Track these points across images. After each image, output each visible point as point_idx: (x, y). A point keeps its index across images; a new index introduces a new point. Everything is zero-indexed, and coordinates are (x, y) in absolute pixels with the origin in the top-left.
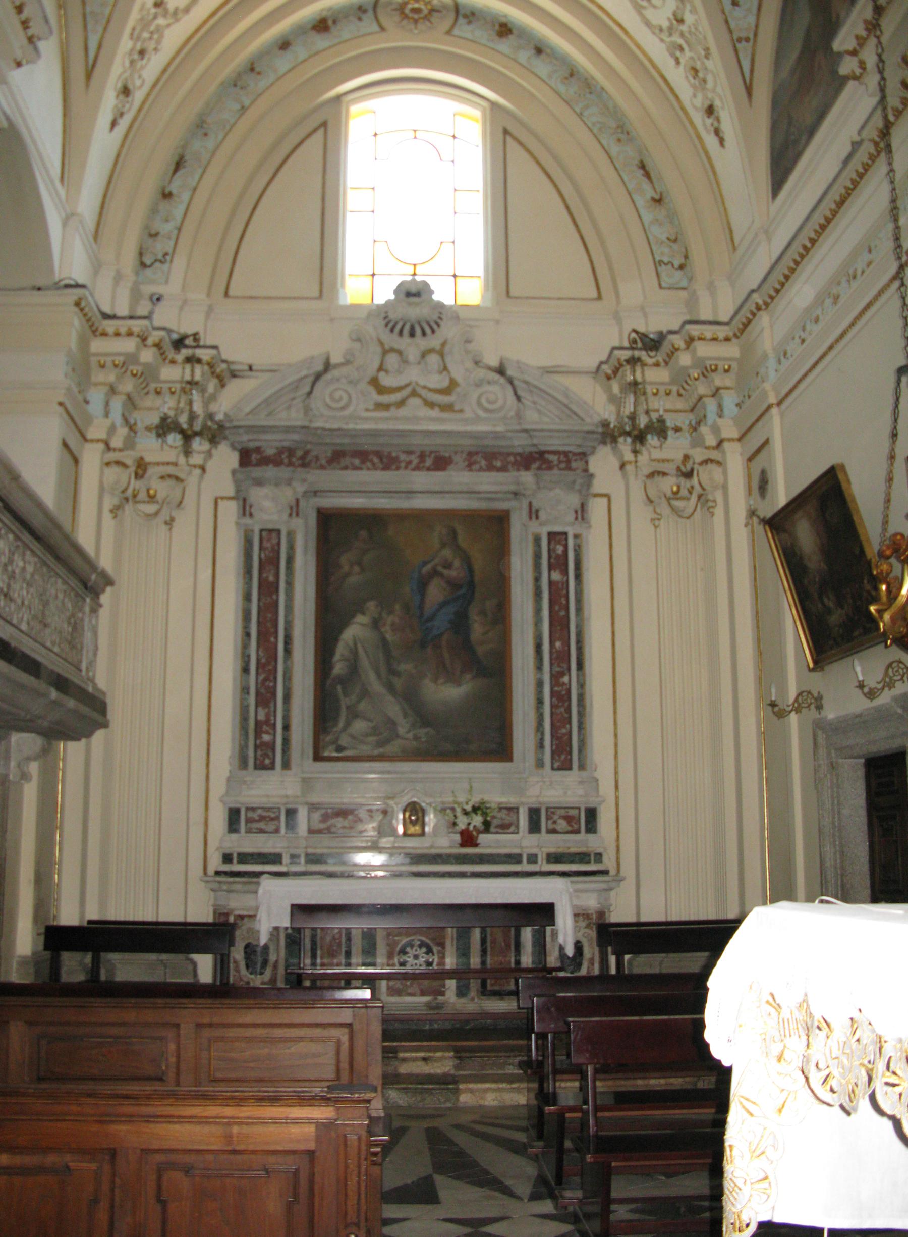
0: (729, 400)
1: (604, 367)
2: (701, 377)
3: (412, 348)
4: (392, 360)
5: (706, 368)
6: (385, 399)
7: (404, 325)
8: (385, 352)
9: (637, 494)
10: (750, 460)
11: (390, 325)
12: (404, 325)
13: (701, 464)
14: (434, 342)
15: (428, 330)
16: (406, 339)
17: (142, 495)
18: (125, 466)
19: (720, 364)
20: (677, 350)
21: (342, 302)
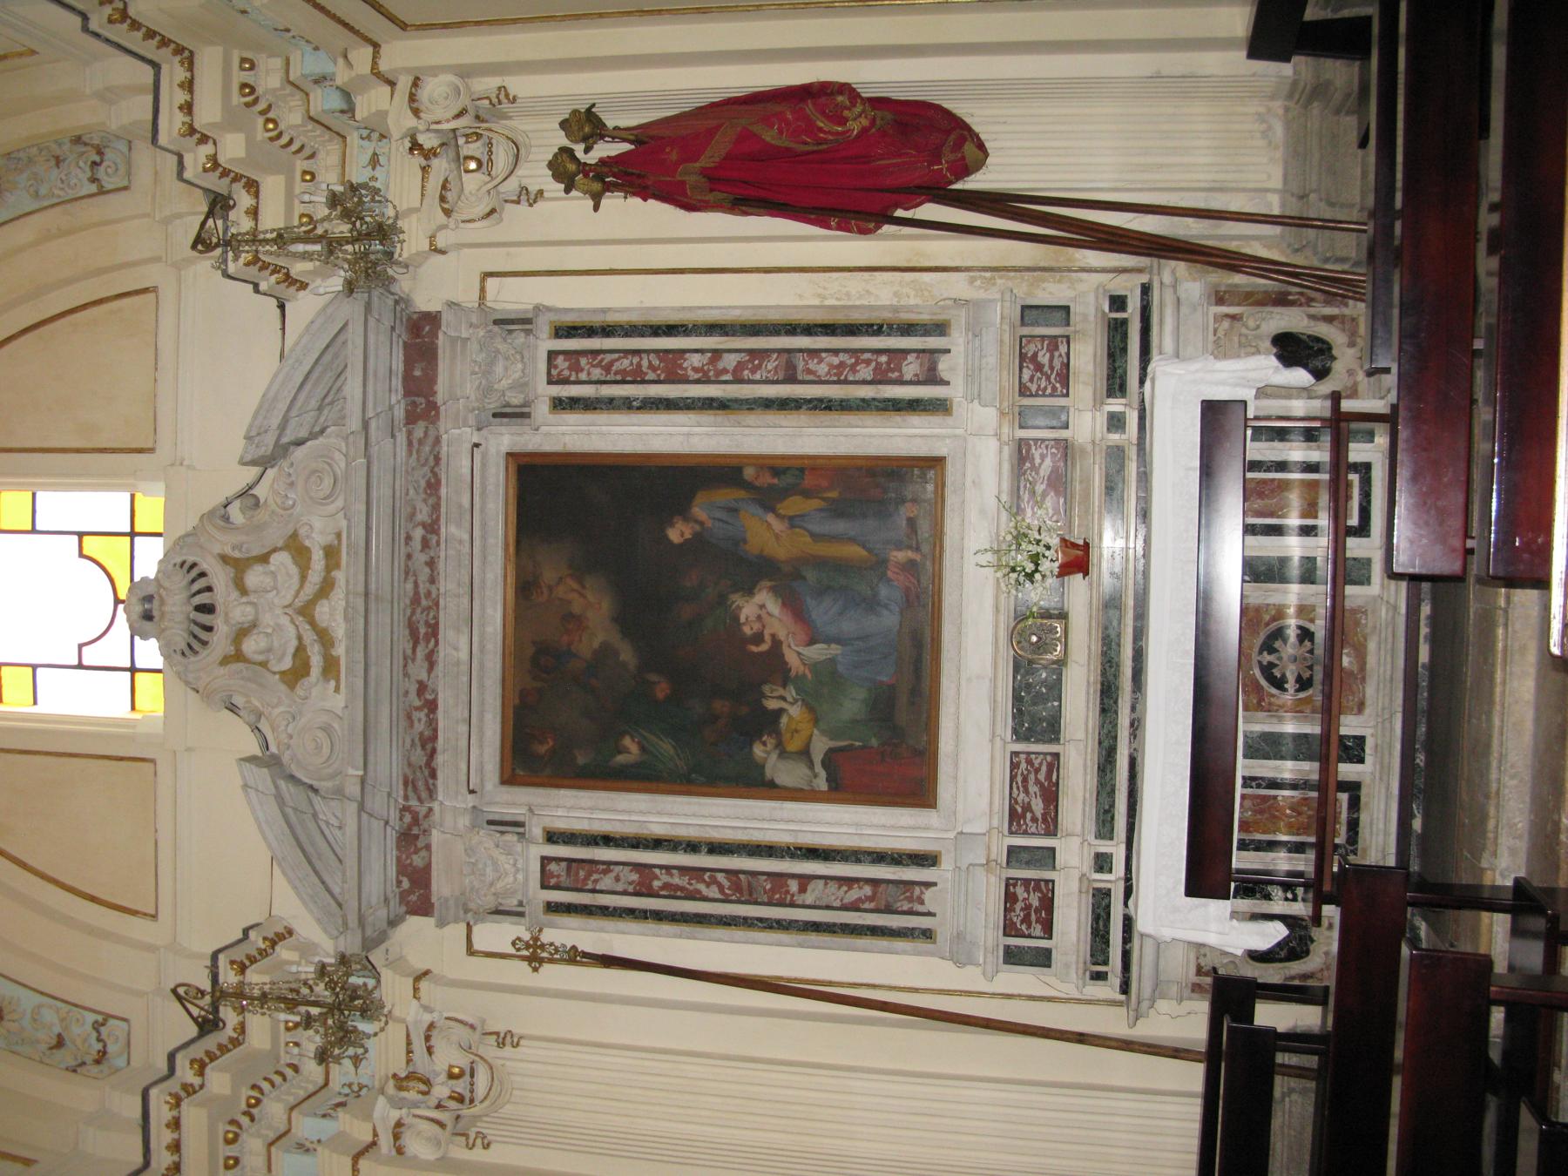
0: (307, 63)
1: (263, 286)
2: (271, 115)
3: (232, 610)
4: (250, 646)
5: (247, 105)
6: (316, 661)
7: (196, 623)
8: (239, 657)
9: (480, 232)
10: (404, 26)
11: (196, 645)
12: (196, 623)
13: (416, 112)
14: (220, 577)
15: (201, 583)
16: (218, 621)
17: (461, 1086)
18: (399, 1124)
19: (239, 77)
20: (214, 159)
21: (159, 728)
